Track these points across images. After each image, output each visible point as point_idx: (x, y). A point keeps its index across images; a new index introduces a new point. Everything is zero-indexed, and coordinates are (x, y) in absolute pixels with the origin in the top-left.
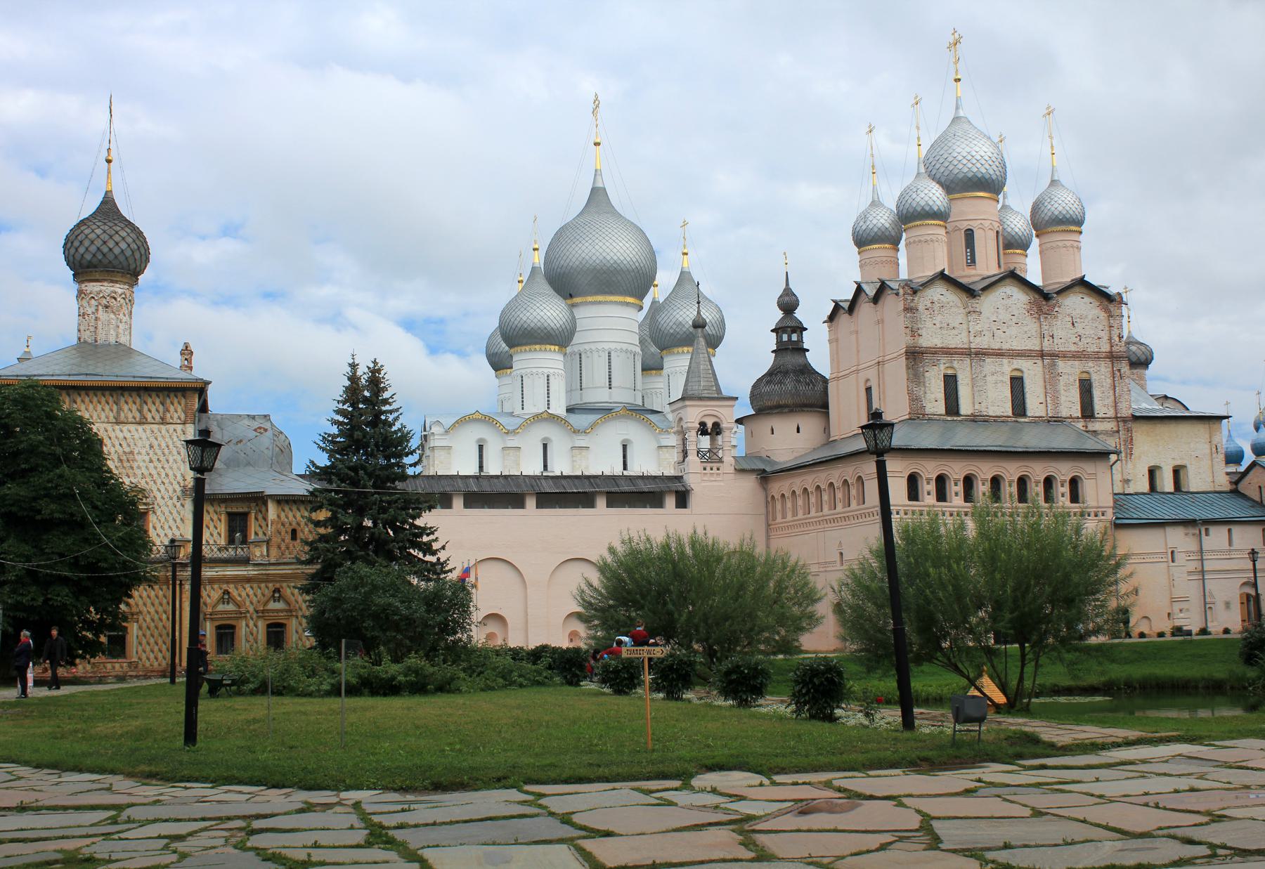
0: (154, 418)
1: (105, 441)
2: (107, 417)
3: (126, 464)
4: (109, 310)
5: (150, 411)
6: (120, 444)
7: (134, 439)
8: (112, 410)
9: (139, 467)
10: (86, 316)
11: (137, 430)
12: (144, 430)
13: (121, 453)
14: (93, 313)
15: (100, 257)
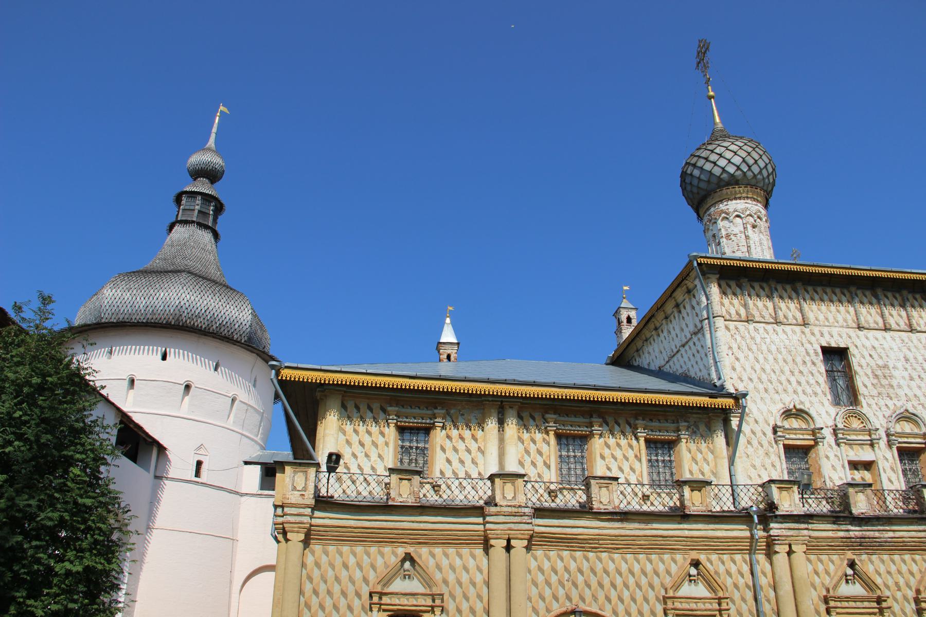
0: (899, 325)
1: (851, 349)
2: (845, 320)
3: (884, 382)
4: (756, 230)
5: (892, 315)
6: (871, 356)
7: (884, 349)
8: (848, 312)
9: (899, 386)
10: (732, 237)
11: (885, 338)
12: (893, 339)
13: (875, 367)
14: (741, 232)
15: (745, 169)
